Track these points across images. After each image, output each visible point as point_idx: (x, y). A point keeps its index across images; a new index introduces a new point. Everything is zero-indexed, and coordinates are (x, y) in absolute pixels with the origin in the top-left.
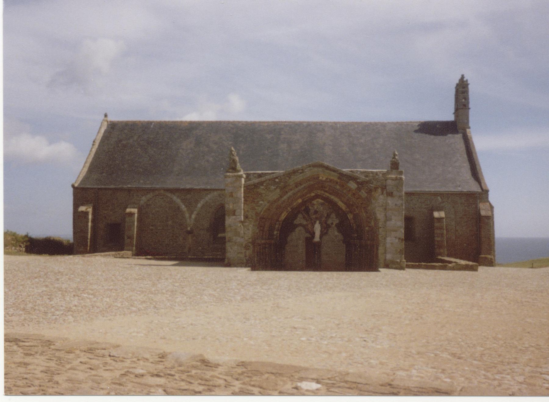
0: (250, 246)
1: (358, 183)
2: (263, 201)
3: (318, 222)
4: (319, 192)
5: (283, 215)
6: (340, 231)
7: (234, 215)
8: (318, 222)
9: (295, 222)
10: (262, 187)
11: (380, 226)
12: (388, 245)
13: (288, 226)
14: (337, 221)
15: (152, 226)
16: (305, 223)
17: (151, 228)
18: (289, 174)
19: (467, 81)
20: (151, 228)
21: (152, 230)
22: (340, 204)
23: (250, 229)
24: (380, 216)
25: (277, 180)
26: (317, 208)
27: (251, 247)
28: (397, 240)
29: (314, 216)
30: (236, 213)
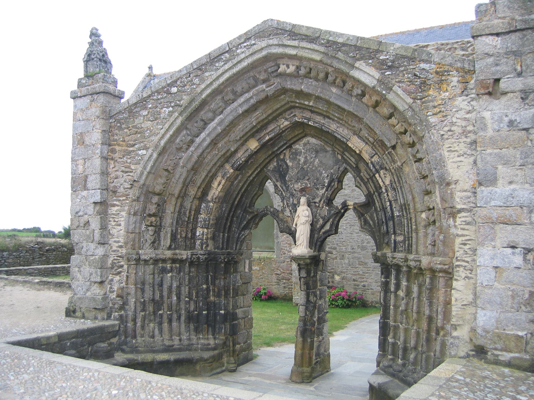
0: (122, 266)
1: (381, 66)
2: (146, 148)
3: (303, 200)
5: (215, 184)
6: (365, 226)
8: (303, 200)
10: (145, 113)
11: (459, 207)
12: (485, 276)
13: (241, 214)
18: (199, 69)
22: (356, 143)
23: (123, 223)
24: (459, 169)
25: (174, 90)
26: (305, 162)
27: (126, 267)
28: (518, 260)
29: (298, 186)
30: (89, 185)
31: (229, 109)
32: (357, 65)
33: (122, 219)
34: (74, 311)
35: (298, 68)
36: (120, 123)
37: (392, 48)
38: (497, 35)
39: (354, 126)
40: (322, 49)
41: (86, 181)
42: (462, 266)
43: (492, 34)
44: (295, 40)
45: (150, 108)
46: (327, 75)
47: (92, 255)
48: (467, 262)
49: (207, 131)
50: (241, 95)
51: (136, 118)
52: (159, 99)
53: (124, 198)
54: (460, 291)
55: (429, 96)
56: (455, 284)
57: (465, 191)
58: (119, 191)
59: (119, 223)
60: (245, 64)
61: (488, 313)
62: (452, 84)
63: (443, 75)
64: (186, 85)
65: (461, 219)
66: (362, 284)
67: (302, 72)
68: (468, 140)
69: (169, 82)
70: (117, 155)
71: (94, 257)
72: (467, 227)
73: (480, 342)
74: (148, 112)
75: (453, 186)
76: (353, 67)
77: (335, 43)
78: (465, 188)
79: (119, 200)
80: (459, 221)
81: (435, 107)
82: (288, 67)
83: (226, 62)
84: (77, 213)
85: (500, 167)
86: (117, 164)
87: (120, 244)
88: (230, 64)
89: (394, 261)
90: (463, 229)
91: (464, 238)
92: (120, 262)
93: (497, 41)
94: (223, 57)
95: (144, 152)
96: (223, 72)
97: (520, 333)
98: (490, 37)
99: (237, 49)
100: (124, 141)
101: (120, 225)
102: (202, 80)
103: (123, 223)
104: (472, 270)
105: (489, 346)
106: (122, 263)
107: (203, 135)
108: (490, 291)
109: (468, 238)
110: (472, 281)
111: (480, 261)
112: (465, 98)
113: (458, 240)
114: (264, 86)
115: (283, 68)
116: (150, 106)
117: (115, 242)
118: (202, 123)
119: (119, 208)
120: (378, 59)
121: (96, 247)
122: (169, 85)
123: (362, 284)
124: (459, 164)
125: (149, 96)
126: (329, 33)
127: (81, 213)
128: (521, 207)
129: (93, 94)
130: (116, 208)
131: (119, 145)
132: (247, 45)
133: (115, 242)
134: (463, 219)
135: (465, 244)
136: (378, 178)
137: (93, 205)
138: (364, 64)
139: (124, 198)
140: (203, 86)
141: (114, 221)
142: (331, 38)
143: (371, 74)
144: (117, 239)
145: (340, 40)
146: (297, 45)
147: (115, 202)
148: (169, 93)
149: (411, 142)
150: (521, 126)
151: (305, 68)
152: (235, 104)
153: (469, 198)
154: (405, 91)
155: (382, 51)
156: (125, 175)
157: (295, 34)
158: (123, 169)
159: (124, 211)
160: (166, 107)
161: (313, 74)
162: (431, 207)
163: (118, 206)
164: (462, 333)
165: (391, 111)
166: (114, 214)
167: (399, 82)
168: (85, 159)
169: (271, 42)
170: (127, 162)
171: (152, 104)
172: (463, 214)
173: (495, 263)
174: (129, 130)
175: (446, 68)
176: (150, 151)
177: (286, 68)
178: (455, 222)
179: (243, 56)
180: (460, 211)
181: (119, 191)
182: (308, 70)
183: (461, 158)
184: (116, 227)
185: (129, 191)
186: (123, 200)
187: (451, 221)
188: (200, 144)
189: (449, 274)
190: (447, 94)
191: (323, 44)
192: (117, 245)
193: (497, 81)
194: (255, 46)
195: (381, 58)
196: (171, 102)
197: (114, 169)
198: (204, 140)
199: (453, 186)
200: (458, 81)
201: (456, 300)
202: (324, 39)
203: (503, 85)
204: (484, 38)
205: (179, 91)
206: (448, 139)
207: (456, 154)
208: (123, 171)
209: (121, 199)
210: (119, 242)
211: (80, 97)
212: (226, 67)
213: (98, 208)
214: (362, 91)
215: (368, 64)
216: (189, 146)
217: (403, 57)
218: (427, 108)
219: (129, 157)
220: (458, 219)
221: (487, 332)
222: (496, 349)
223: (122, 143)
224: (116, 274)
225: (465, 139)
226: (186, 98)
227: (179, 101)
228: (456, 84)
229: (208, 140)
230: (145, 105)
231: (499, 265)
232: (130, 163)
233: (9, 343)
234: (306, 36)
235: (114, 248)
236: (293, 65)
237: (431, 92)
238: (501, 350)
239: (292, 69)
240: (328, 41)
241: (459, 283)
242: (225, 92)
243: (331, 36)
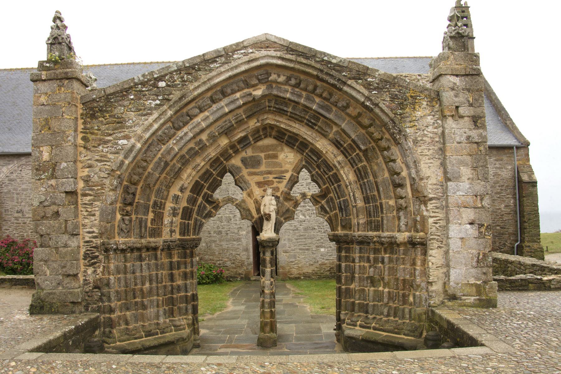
0: (97, 257)
1: (368, 86)
2: (127, 137)
4: (271, 119)
7: (53, 176)
9: (218, 195)
11: (431, 196)
14: (314, 189)
15: (18, 212)
16: (239, 195)
17: (16, 215)
19: (466, 3)
20: (16, 215)
21: (17, 219)
25: (162, 84)
27: (101, 257)
32: (349, 82)
33: (97, 209)
34: (42, 308)
35: (289, 79)
36: (94, 111)
37: (377, 73)
38: (457, 76)
39: (327, 132)
40: (318, 66)
41: (54, 169)
42: (435, 239)
43: (453, 75)
44: (292, 55)
45: (132, 99)
46: (316, 87)
47: (64, 247)
48: (439, 236)
49: (190, 126)
50: (229, 95)
51: (115, 108)
52: (143, 91)
53: (100, 188)
54: (435, 256)
55: (407, 113)
56: (430, 252)
57: (435, 184)
58: (93, 180)
59: (93, 213)
60: (243, 68)
61: (458, 271)
62: (423, 106)
63: (416, 99)
64: (176, 81)
65: (432, 205)
66: (218, 262)
67: (293, 82)
68: (436, 148)
69: (156, 76)
70: (90, 143)
71: (66, 249)
72: (437, 210)
73: (450, 292)
74: (130, 103)
75: (425, 181)
76: (345, 83)
77: (330, 63)
78: (435, 182)
79: (94, 190)
80: (430, 206)
81: (411, 122)
83: (223, 64)
84: (41, 203)
85: (462, 168)
86: (89, 153)
87: (94, 234)
88: (226, 67)
89: (360, 238)
90: (435, 212)
91: (435, 219)
92: (95, 253)
93: (457, 80)
94: (217, 60)
95: (125, 142)
96: (220, 74)
97: (478, 283)
98: (452, 76)
99: (233, 54)
100: (99, 130)
101: (94, 215)
102: (196, 79)
103: (98, 213)
104: (442, 242)
105: (459, 294)
106: (97, 254)
107: (185, 129)
108: (458, 256)
109: (438, 218)
110: (443, 249)
111: (451, 234)
112: (432, 117)
113: (431, 220)
114: (251, 90)
115: (273, 77)
116: (132, 97)
117: (89, 232)
118: (188, 118)
119: (92, 197)
120: (366, 80)
121: (69, 238)
122: (155, 79)
123: (218, 262)
124: (430, 165)
125: (131, 88)
126: (325, 54)
127: (46, 203)
128: (476, 196)
129: (62, 79)
130: (89, 198)
131: (92, 133)
132: (245, 53)
133: (89, 232)
134: (434, 205)
135: (436, 223)
136: (343, 174)
137: (65, 194)
138: (355, 83)
139: (100, 188)
140: (196, 84)
141: (87, 211)
142: (326, 58)
143: (361, 91)
144: (91, 230)
145: (334, 61)
146: (294, 59)
147: (87, 192)
148: (155, 86)
149: (387, 146)
150: (474, 140)
151: (296, 79)
153: (438, 189)
154: (388, 107)
155: (369, 75)
156: (99, 164)
157: (292, 50)
158: (97, 158)
159: (98, 201)
160: (152, 100)
161: (302, 86)
162: (404, 196)
163: (91, 195)
164: (437, 287)
165: (371, 122)
166: (85, 204)
167: (384, 100)
168: (52, 146)
169: (269, 53)
170: (102, 151)
171: (135, 95)
172: (434, 201)
173: (461, 235)
174: (105, 119)
175: (418, 94)
176: (133, 140)
178: (426, 206)
179: (240, 62)
180: (431, 199)
181: (93, 180)
182: (298, 81)
183: (431, 161)
184: (88, 217)
185: (105, 180)
186: (98, 190)
187: (423, 207)
188: (181, 138)
189: (424, 245)
190: (420, 113)
191: (318, 61)
192: (90, 235)
193: (457, 107)
194: (252, 55)
195: (369, 80)
196: (157, 96)
197: (86, 158)
198: (186, 134)
199: (425, 181)
200: (427, 105)
201: (433, 264)
202: (319, 58)
203: (461, 110)
204: (448, 77)
205: (168, 85)
206: (420, 146)
207: (427, 157)
208: (97, 160)
209: (96, 188)
210: (93, 232)
211: (45, 80)
212: (222, 69)
213: (69, 197)
214: (347, 104)
215: (358, 83)
216: (170, 138)
217: (386, 81)
218: (405, 122)
219: (105, 146)
220: (428, 205)
221: (458, 284)
222: (464, 295)
223: (96, 131)
224: (90, 266)
225: (433, 147)
226: (176, 95)
227: (167, 95)
228: (426, 106)
229: (191, 135)
230: (125, 95)
231: (463, 236)
232: (107, 152)
233: (38, 349)
234: (302, 53)
235: (87, 239)
236: (284, 76)
237: (407, 110)
238: (467, 296)
239: (282, 79)
240: (323, 60)
241: (434, 251)
242: (222, 91)
243: (325, 56)
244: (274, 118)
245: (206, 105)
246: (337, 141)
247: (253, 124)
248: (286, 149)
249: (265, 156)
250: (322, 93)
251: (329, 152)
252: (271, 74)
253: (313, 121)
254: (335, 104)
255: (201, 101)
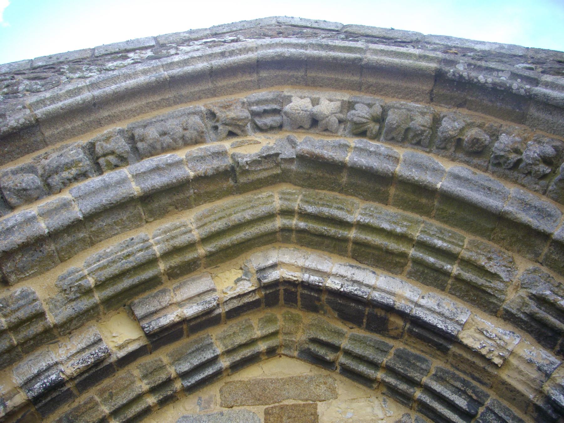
4: (292, 263)
31: (95, 181)
39: (495, 276)
82: (315, 102)
114: (227, 145)
151: (370, 106)
152: (125, 172)
177: (310, 106)
244: (301, 262)
245: (67, 166)
246: (541, 300)
247: (230, 283)
248: (344, 387)
249: (267, 413)
250: (462, 130)
251: (514, 361)
252: (290, 97)
253: (439, 243)
254: (514, 157)
255: (54, 155)
